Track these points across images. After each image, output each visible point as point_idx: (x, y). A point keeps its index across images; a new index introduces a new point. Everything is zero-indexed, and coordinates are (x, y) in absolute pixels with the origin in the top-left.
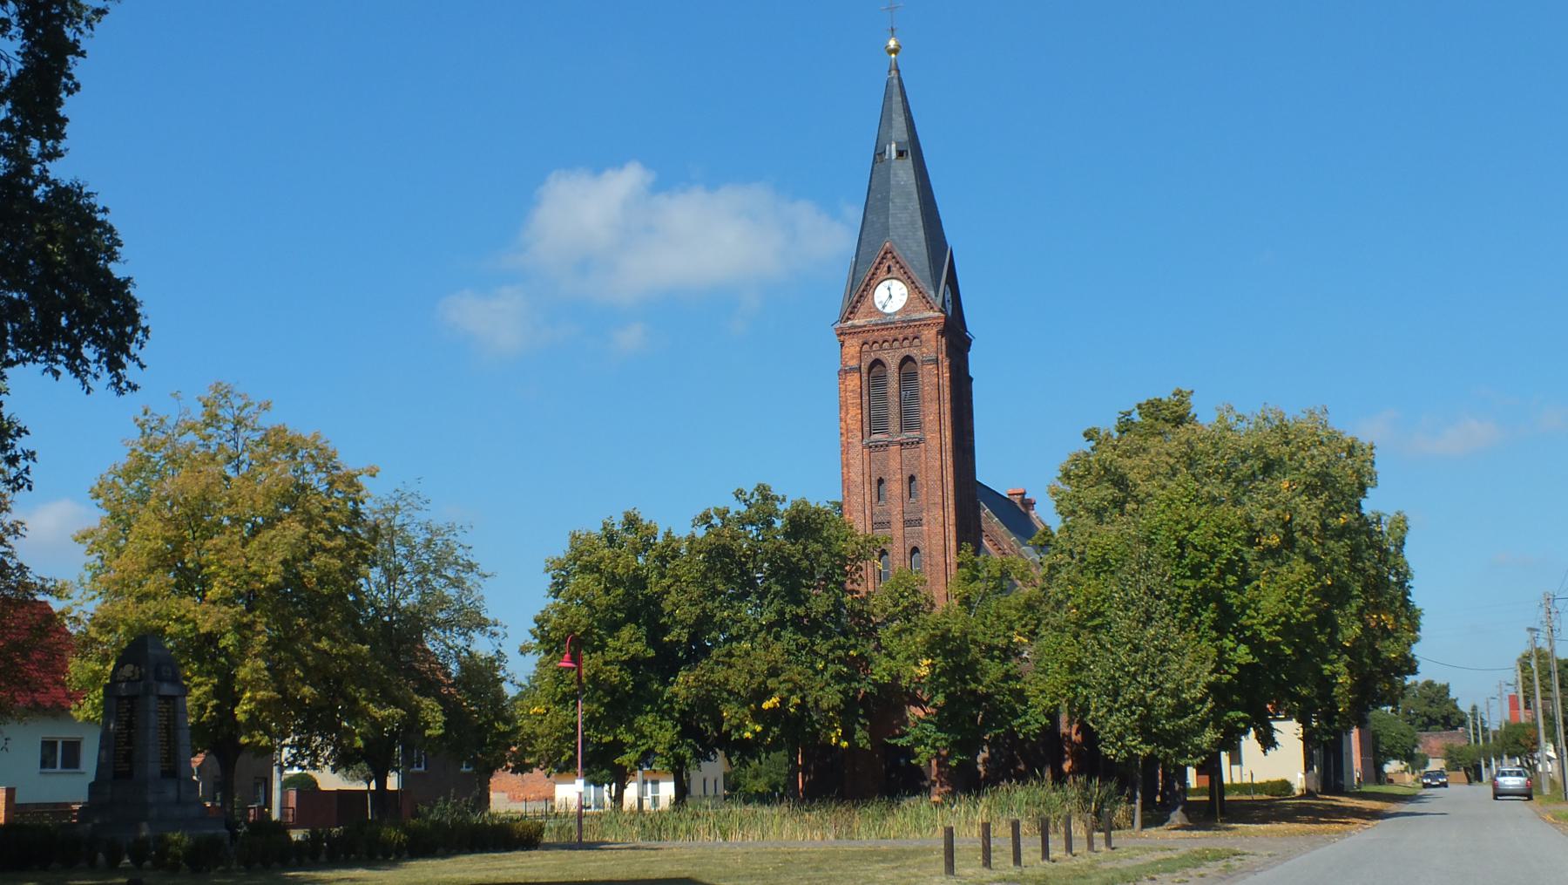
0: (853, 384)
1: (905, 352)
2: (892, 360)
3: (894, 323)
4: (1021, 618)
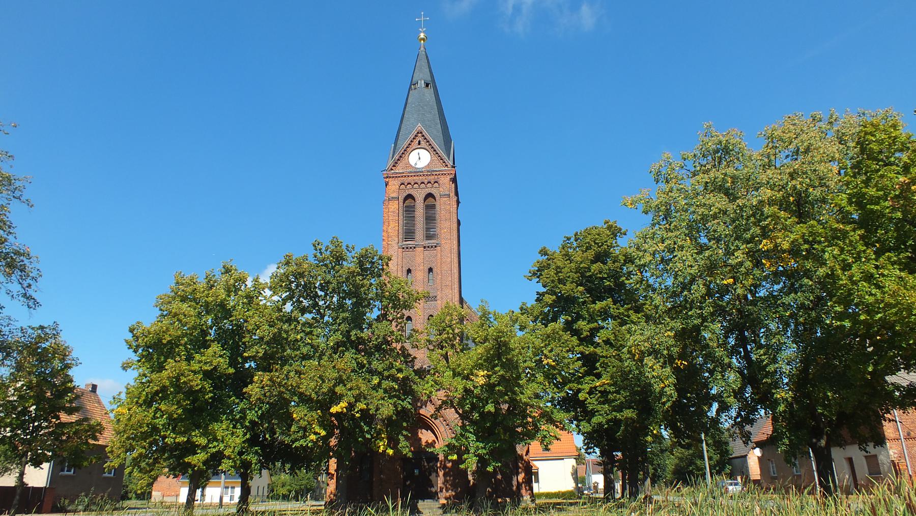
0: (393, 207)
1: (428, 191)
2: (419, 195)
3: (422, 172)
4: (546, 346)
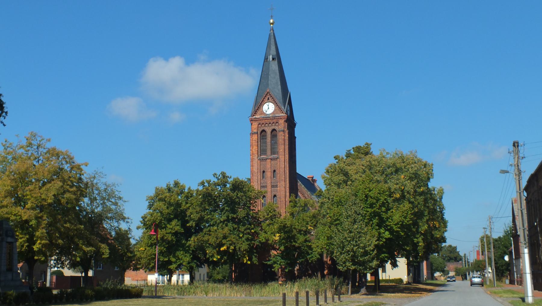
1: (273, 127)
2: (268, 130)
3: (269, 117)
4: (311, 221)
